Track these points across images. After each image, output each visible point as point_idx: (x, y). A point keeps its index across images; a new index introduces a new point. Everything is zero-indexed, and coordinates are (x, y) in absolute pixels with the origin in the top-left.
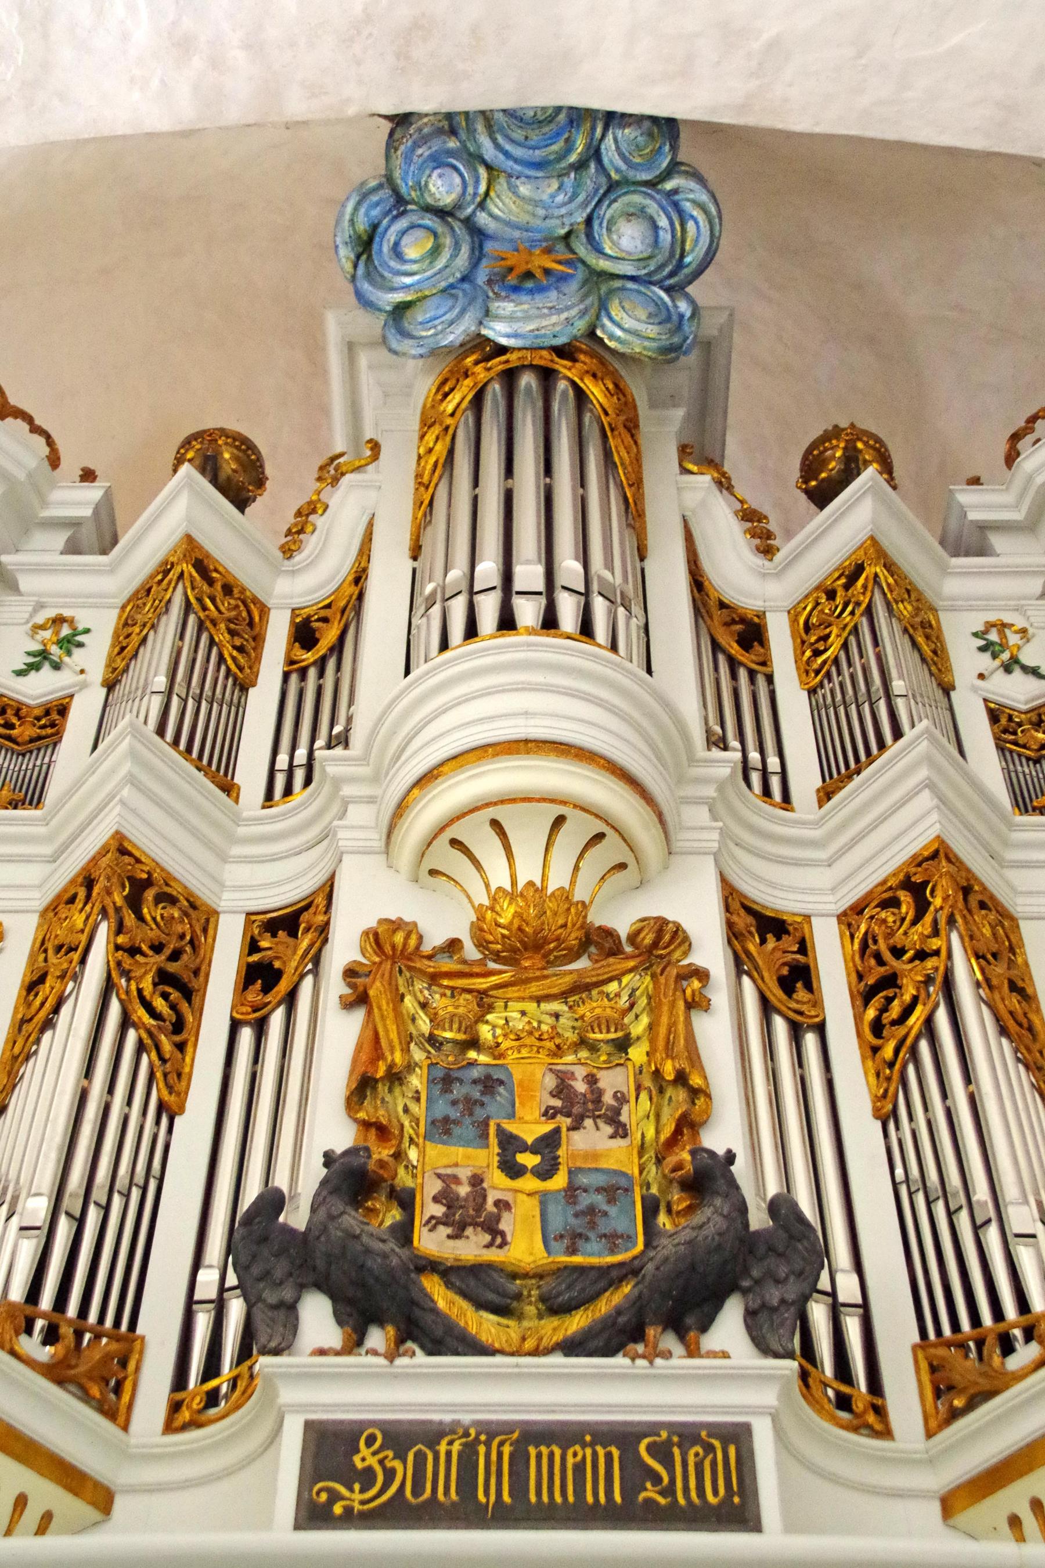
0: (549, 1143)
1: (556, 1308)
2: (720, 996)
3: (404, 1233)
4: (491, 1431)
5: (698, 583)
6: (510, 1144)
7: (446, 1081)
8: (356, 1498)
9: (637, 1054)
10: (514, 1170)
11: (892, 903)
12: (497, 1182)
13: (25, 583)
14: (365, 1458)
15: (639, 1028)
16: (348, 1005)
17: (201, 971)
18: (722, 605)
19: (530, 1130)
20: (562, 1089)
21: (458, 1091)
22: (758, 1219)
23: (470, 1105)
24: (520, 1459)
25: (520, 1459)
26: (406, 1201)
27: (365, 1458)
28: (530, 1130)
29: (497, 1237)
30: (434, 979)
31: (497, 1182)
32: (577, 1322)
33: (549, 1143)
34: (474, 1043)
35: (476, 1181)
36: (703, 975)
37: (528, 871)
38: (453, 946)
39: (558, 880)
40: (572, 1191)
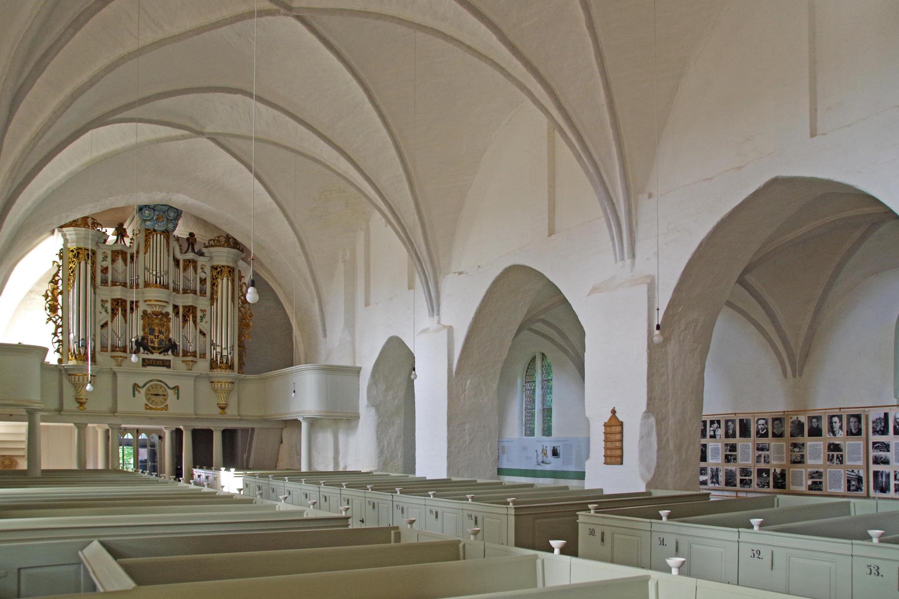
0: (158, 336)
1: (158, 350)
2: (171, 321)
3: (147, 343)
4: (154, 359)
5: (174, 256)
6: (155, 336)
7: (150, 329)
8: (145, 364)
9: (165, 327)
10: (155, 338)
11: (187, 308)
12: (154, 339)
13: (101, 247)
14: (146, 361)
15: (165, 324)
16: (142, 319)
17: (127, 308)
18: (176, 259)
19: (157, 334)
20: (159, 331)
21: (151, 330)
22: (173, 343)
23: (152, 332)
24: (156, 362)
25: (156, 362)
26: (147, 340)
27: (146, 361)
28: (157, 334)
29: (154, 344)
30: (149, 318)
31: (154, 339)
32: (160, 351)
33: (158, 336)
34: (152, 324)
35: (153, 339)
36: (170, 318)
37: (157, 310)
38: (150, 314)
39: (160, 310)
40: (160, 340)
